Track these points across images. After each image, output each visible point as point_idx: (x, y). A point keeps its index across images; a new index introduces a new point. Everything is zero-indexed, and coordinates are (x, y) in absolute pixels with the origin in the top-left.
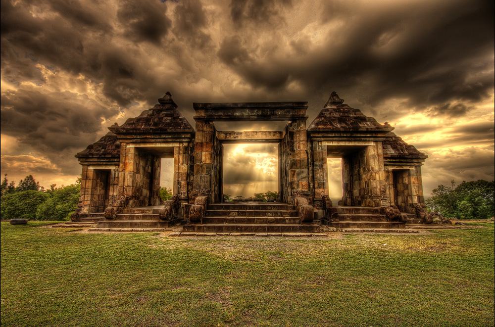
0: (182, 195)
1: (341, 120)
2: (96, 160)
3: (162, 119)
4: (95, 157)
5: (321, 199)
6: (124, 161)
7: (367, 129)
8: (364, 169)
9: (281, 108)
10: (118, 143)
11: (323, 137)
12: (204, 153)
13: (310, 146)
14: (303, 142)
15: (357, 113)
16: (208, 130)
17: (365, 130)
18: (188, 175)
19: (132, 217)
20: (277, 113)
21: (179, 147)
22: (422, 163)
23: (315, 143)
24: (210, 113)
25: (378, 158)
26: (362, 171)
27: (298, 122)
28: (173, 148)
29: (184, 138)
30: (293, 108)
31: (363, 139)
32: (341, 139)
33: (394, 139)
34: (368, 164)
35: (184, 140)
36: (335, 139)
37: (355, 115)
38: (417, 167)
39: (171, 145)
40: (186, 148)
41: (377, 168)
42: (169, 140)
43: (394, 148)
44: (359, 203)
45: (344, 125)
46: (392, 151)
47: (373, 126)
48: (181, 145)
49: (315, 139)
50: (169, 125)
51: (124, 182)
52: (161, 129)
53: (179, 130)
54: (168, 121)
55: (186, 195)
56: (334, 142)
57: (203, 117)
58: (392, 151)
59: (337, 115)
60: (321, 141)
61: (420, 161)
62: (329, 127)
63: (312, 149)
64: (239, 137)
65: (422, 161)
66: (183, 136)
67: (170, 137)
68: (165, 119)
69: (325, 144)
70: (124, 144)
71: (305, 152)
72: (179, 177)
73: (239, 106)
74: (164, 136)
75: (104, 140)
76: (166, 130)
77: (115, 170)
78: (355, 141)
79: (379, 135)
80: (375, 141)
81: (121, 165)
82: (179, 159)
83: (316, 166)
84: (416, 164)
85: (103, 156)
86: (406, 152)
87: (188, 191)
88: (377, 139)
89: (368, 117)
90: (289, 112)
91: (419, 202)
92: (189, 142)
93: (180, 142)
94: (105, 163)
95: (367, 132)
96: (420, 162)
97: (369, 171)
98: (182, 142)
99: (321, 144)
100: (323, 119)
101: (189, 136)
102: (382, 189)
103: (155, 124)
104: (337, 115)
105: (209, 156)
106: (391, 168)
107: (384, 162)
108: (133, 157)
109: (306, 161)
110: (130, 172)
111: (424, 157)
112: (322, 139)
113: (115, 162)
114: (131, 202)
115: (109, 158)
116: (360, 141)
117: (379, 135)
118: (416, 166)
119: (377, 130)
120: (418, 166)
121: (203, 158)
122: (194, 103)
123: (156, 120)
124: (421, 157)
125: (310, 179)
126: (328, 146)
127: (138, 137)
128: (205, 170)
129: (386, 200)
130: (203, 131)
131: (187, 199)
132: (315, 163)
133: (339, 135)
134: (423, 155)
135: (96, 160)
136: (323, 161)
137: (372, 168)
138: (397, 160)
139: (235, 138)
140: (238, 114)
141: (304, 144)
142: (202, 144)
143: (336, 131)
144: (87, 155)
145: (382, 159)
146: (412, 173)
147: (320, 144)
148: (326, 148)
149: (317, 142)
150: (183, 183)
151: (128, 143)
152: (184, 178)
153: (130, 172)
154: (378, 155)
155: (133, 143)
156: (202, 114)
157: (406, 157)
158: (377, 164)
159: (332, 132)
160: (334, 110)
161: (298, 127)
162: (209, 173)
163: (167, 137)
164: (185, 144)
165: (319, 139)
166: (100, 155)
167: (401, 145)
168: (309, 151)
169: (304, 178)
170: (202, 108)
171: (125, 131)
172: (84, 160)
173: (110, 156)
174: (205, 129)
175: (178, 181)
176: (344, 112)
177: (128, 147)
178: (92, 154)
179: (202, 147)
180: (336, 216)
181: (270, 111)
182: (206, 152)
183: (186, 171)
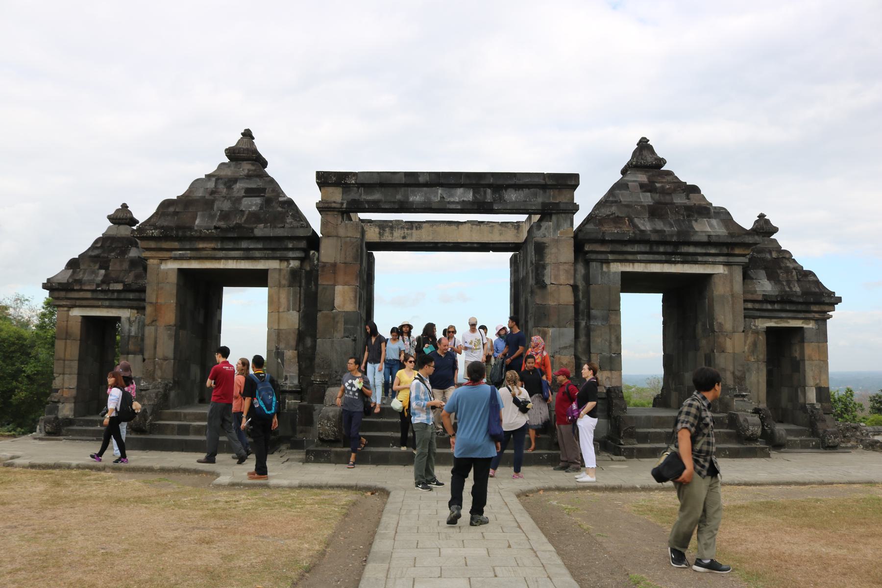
0: (288, 382)
1: (654, 212)
2: (89, 295)
3: (240, 203)
4: (86, 288)
5: (604, 396)
6: (154, 301)
7: (709, 236)
8: (704, 325)
9: (518, 187)
10: (133, 253)
11: (612, 252)
12: (339, 289)
13: (583, 271)
14: (566, 267)
15: (691, 195)
16: (349, 235)
17: (705, 239)
18: (301, 336)
19: (184, 430)
20: (506, 197)
21: (280, 270)
22: (830, 313)
23: (593, 265)
24: (354, 195)
25: (733, 304)
26: (699, 330)
27: (554, 218)
29: (292, 249)
30: (544, 187)
31: (700, 259)
32: (651, 257)
33: (774, 255)
34: (712, 318)
35: (291, 254)
36: (639, 257)
37: (686, 201)
38: (820, 322)
40: (294, 275)
41: (728, 326)
42: (257, 254)
45: (660, 225)
46: (765, 286)
48: (284, 265)
49: (594, 256)
50: (255, 218)
51: (155, 348)
52: (238, 227)
53: (279, 232)
54: (254, 208)
55: (296, 382)
56: (636, 265)
57: (338, 206)
58: (765, 286)
59: (647, 199)
60: (608, 262)
61: (826, 308)
62: (625, 229)
63: (587, 278)
64: (414, 235)
65: (831, 308)
66: (290, 246)
67: (260, 246)
68: (246, 201)
69: (618, 268)
70: (156, 261)
71: (570, 288)
72: (279, 340)
73: (421, 180)
74: (244, 245)
75: (102, 247)
76: (252, 229)
77: (129, 319)
78: (683, 262)
79: (737, 251)
80: (726, 264)
81: (149, 310)
82: (279, 299)
83: (595, 318)
84: (817, 316)
85: (105, 287)
86: (797, 289)
87: (301, 373)
88: (732, 259)
89: (715, 208)
90: (535, 195)
91: (819, 400)
92: (302, 260)
93: (282, 259)
94: (107, 303)
95: (709, 244)
96: (826, 312)
97: (713, 331)
98: (287, 259)
99: (608, 267)
100: (614, 209)
101: (303, 244)
102: (737, 373)
103: (225, 216)
104: (647, 199)
105: (351, 295)
106: (763, 324)
107: (745, 309)
108: (175, 292)
109: (571, 309)
110: (168, 327)
111: (833, 300)
112: (610, 257)
113: (130, 300)
114: (172, 394)
115: (118, 291)
116: (696, 262)
117: (737, 251)
118: (816, 320)
119: (729, 240)
120: (823, 320)
121: (338, 301)
122: (318, 173)
123: (226, 206)
124: (827, 300)
125: (580, 348)
126: (623, 273)
127: (188, 247)
128: (341, 326)
129: (743, 396)
130: (337, 236)
131: (298, 393)
132: (593, 312)
133: (647, 249)
134: (831, 294)
135: (89, 295)
136: (614, 309)
137: (720, 325)
138: (776, 307)
139: (404, 237)
141: (567, 271)
142: (334, 265)
143: (641, 239)
144: (68, 283)
145: (740, 306)
146: (807, 335)
147: (605, 269)
148: (619, 278)
149: (599, 264)
151: (162, 260)
152: (293, 343)
153: (168, 327)
154: (733, 295)
155: (175, 259)
156: (337, 196)
157: (795, 299)
158: (729, 317)
159: (632, 242)
160: (642, 186)
161: (555, 231)
162: (348, 333)
163: (252, 246)
164: (294, 264)
165: (603, 257)
166: (98, 285)
167: (788, 271)
168: (581, 284)
169: (565, 348)
170: (336, 184)
171: (156, 233)
172: (62, 294)
173: (119, 287)
174: (342, 232)
175: (277, 349)
176: (663, 192)
177: (163, 267)
178: (79, 282)
179: (334, 273)
180: (632, 435)
181: (494, 192)
182: (345, 284)
183: (297, 327)
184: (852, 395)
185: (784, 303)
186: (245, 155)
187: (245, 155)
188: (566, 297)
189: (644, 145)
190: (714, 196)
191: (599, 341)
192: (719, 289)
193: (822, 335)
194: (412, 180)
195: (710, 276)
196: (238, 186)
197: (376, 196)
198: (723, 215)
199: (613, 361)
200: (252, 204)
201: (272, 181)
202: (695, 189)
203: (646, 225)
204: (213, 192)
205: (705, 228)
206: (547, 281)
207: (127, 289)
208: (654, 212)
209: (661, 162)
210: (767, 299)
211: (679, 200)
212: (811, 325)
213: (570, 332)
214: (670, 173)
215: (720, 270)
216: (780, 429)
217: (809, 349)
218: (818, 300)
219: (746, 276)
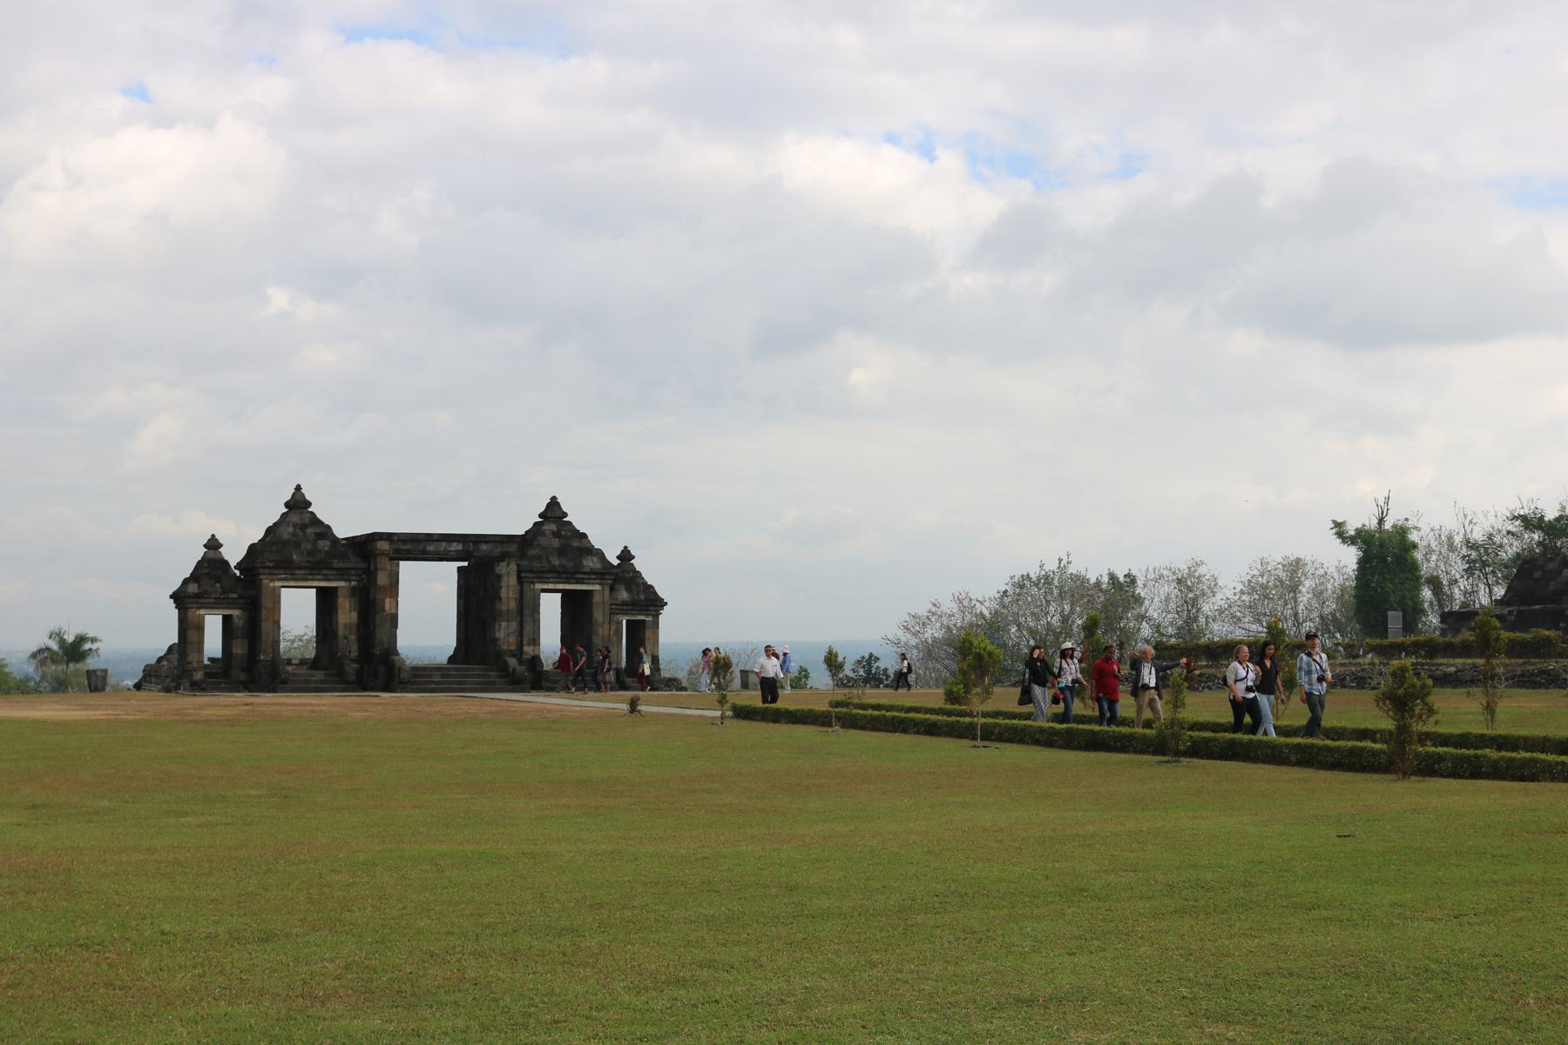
1: (561, 552)
18: (359, 625)
28: (336, 588)
39: (333, 584)
43: (628, 589)
44: (582, 667)
45: (564, 562)
46: (624, 595)
47: (599, 566)
58: (624, 595)
59: (556, 543)
69: (539, 586)
93: (349, 581)
103: (310, 553)
104: (556, 543)
120: (656, 616)
121: (387, 607)
123: (309, 546)
140: (431, 548)
143: (553, 570)
150: (353, 637)
167: (638, 585)
178: (206, 592)
184: (806, 677)
185: (633, 606)
186: (298, 503)
187: (298, 503)
188: (513, 605)
189: (554, 504)
190: (596, 541)
191: (528, 629)
192: (597, 599)
193: (656, 625)
194: (429, 537)
195: (590, 592)
196: (309, 531)
197: (408, 547)
198: (600, 554)
199: (535, 641)
200: (324, 545)
201: (329, 527)
202: (584, 536)
203: (556, 562)
204: (294, 535)
205: (590, 563)
206: (503, 595)
207: (240, 597)
208: (561, 552)
209: (565, 515)
210: (624, 603)
211: (575, 544)
212: (650, 619)
213: (514, 625)
214: (569, 523)
215: (597, 587)
216: (629, 680)
217: (648, 633)
218: (652, 603)
219: (612, 589)
